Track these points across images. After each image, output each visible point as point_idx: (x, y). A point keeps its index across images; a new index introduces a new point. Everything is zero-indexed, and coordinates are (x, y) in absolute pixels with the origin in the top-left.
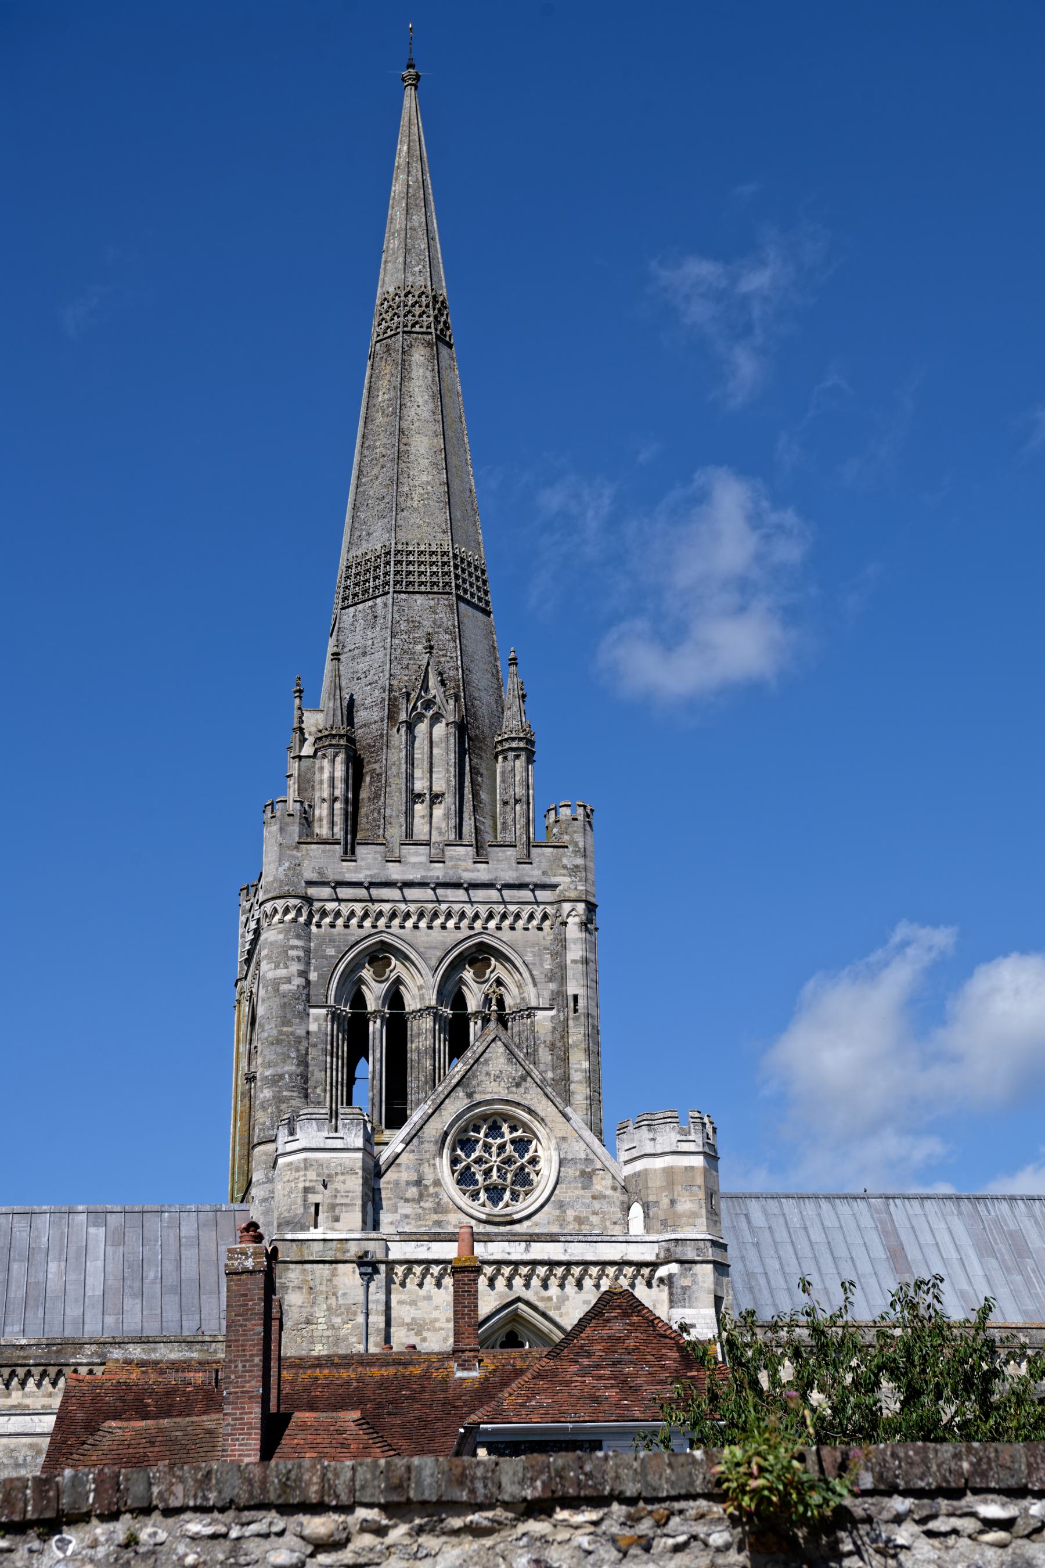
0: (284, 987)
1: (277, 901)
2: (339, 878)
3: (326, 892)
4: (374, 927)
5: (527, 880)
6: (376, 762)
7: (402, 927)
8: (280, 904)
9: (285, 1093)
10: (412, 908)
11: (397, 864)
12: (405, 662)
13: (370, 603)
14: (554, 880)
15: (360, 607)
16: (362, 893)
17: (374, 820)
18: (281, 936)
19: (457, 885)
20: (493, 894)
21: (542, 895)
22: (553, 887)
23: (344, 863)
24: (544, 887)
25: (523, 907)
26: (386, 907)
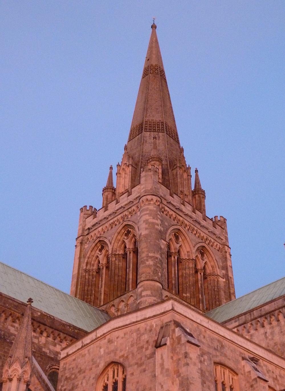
0: (156, 226)
1: (153, 196)
3: (165, 202)
9: (158, 265)
10: (188, 223)
13: (157, 133)
15: (152, 133)
18: (155, 209)
24: (219, 238)
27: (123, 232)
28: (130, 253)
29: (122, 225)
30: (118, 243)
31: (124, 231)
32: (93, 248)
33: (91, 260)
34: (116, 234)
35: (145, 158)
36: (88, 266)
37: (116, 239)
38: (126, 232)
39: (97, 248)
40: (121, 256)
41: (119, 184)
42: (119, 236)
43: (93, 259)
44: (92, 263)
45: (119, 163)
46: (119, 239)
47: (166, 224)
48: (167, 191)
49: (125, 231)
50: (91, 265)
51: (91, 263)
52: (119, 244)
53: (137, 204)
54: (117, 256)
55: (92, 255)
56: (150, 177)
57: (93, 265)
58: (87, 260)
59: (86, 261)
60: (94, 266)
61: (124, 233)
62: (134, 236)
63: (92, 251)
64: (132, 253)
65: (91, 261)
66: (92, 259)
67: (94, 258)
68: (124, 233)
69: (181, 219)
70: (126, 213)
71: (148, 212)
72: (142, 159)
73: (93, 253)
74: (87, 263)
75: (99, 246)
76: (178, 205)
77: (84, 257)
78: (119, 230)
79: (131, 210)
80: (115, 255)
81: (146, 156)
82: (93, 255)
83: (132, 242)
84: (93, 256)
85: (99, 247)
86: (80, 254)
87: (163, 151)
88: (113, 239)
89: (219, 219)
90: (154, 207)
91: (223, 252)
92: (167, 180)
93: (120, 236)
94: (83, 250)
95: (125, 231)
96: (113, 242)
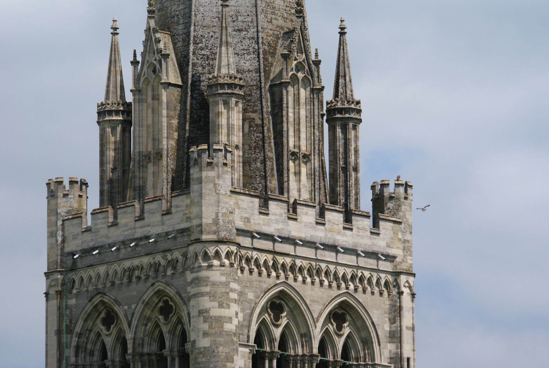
2: (258, 228)
4: (278, 277)
5: (375, 249)
6: (254, 112)
7: (295, 280)
8: (224, 249)
10: (305, 263)
11: (295, 222)
12: (269, 16)
14: (392, 252)
16: (267, 245)
17: (258, 169)
19: (333, 248)
20: (350, 259)
21: (385, 266)
22: (390, 258)
23: (262, 217)
25: (372, 273)
26: (288, 260)
27: (156, 301)
28: (173, 360)
29: (152, 288)
30: (146, 325)
31: (157, 300)
32: (89, 315)
33: (85, 340)
34: (140, 307)
35: (202, 49)
36: (80, 356)
37: (140, 317)
38: (161, 304)
39: (97, 314)
40: (154, 357)
41: (139, 126)
42: (147, 310)
43: (90, 338)
44: (89, 346)
45: (135, 51)
46: (148, 315)
47: (251, 296)
48: (253, 202)
49: (159, 301)
50: (85, 351)
51: (86, 348)
52: (148, 327)
53: (184, 250)
54: (146, 358)
55: (87, 329)
56: (212, 185)
57: (92, 354)
58: (78, 342)
59: (74, 343)
60: (93, 355)
61: (157, 304)
62: (180, 321)
63: (86, 320)
64: (177, 360)
65: (86, 343)
66: (88, 338)
67: (92, 335)
68: (157, 304)
69: (288, 260)
70: (159, 258)
71: (207, 289)
72: (194, 53)
73: (90, 324)
74: (77, 348)
75: (103, 310)
76: (280, 226)
77: (70, 331)
78: (146, 297)
79: (172, 259)
80: (142, 355)
81: (204, 40)
82: (89, 328)
83: (177, 333)
84: (90, 331)
85: (100, 314)
86: (60, 322)
87: (249, 19)
88: (135, 315)
89: (391, 189)
90: (222, 274)
91: (395, 292)
92: (257, 125)
93: (149, 309)
94: (64, 312)
95: (159, 301)
96: (134, 323)
